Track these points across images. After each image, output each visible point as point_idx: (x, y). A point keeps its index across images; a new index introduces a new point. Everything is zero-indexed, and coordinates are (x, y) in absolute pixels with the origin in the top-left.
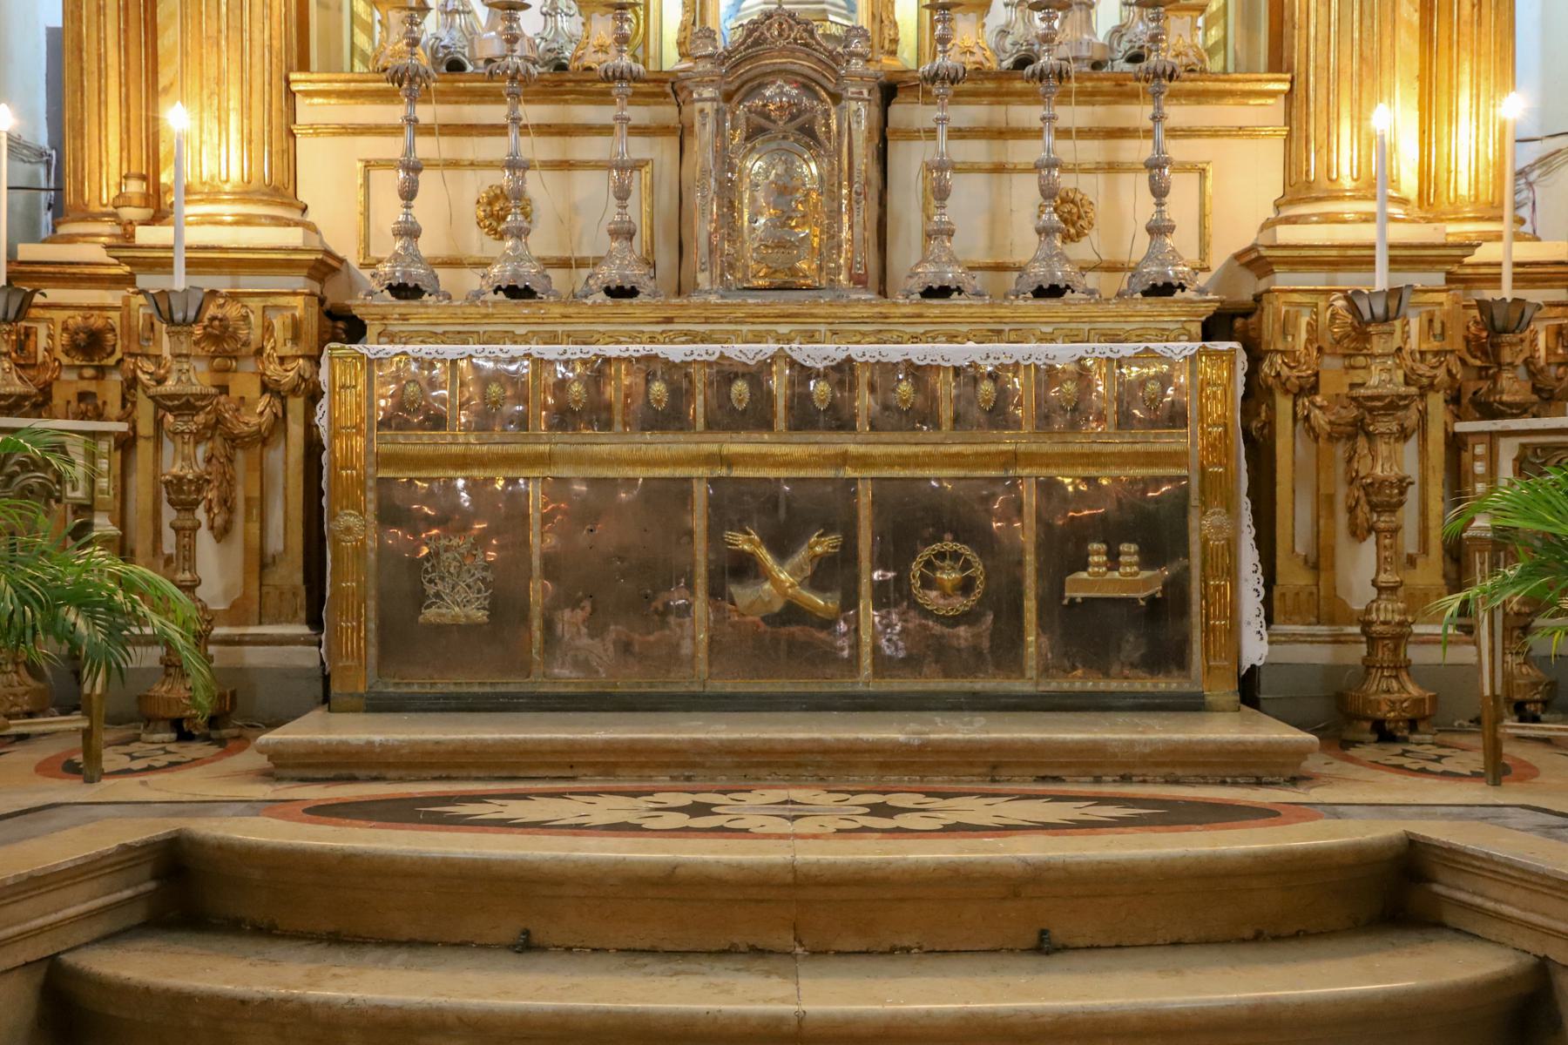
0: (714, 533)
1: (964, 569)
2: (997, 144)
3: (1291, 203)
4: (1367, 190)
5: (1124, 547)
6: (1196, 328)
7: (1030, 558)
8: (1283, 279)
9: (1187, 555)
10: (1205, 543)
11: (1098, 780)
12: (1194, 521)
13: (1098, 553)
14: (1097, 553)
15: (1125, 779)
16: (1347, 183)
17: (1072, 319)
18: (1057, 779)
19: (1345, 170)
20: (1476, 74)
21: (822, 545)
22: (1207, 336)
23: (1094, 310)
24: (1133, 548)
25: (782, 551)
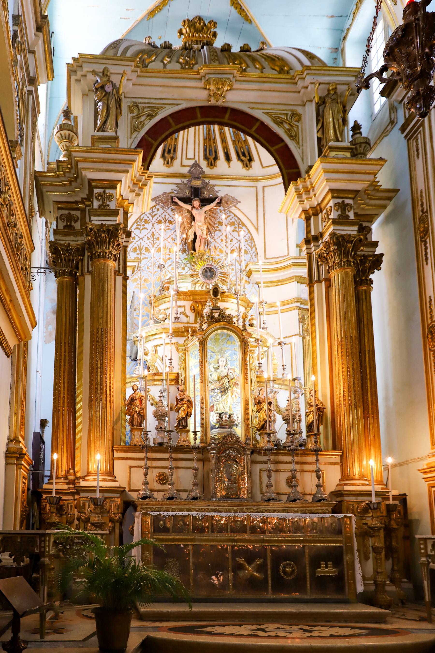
0: (233, 559)
1: (292, 568)
2: (276, 465)
3: (344, 480)
4: (362, 477)
5: (329, 563)
6: (330, 510)
7: (307, 565)
8: (346, 498)
9: (343, 565)
10: (347, 562)
11: (339, 622)
12: (344, 557)
13: (323, 564)
14: (323, 564)
15: (346, 622)
16: (357, 476)
17: (302, 507)
18: (330, 621)
19: (357, 473)
20: (375, 451)
21: (259, 562)
22: (334, 512)
23: (308, 505)
24: (331, 563)
25: (249, 564)
